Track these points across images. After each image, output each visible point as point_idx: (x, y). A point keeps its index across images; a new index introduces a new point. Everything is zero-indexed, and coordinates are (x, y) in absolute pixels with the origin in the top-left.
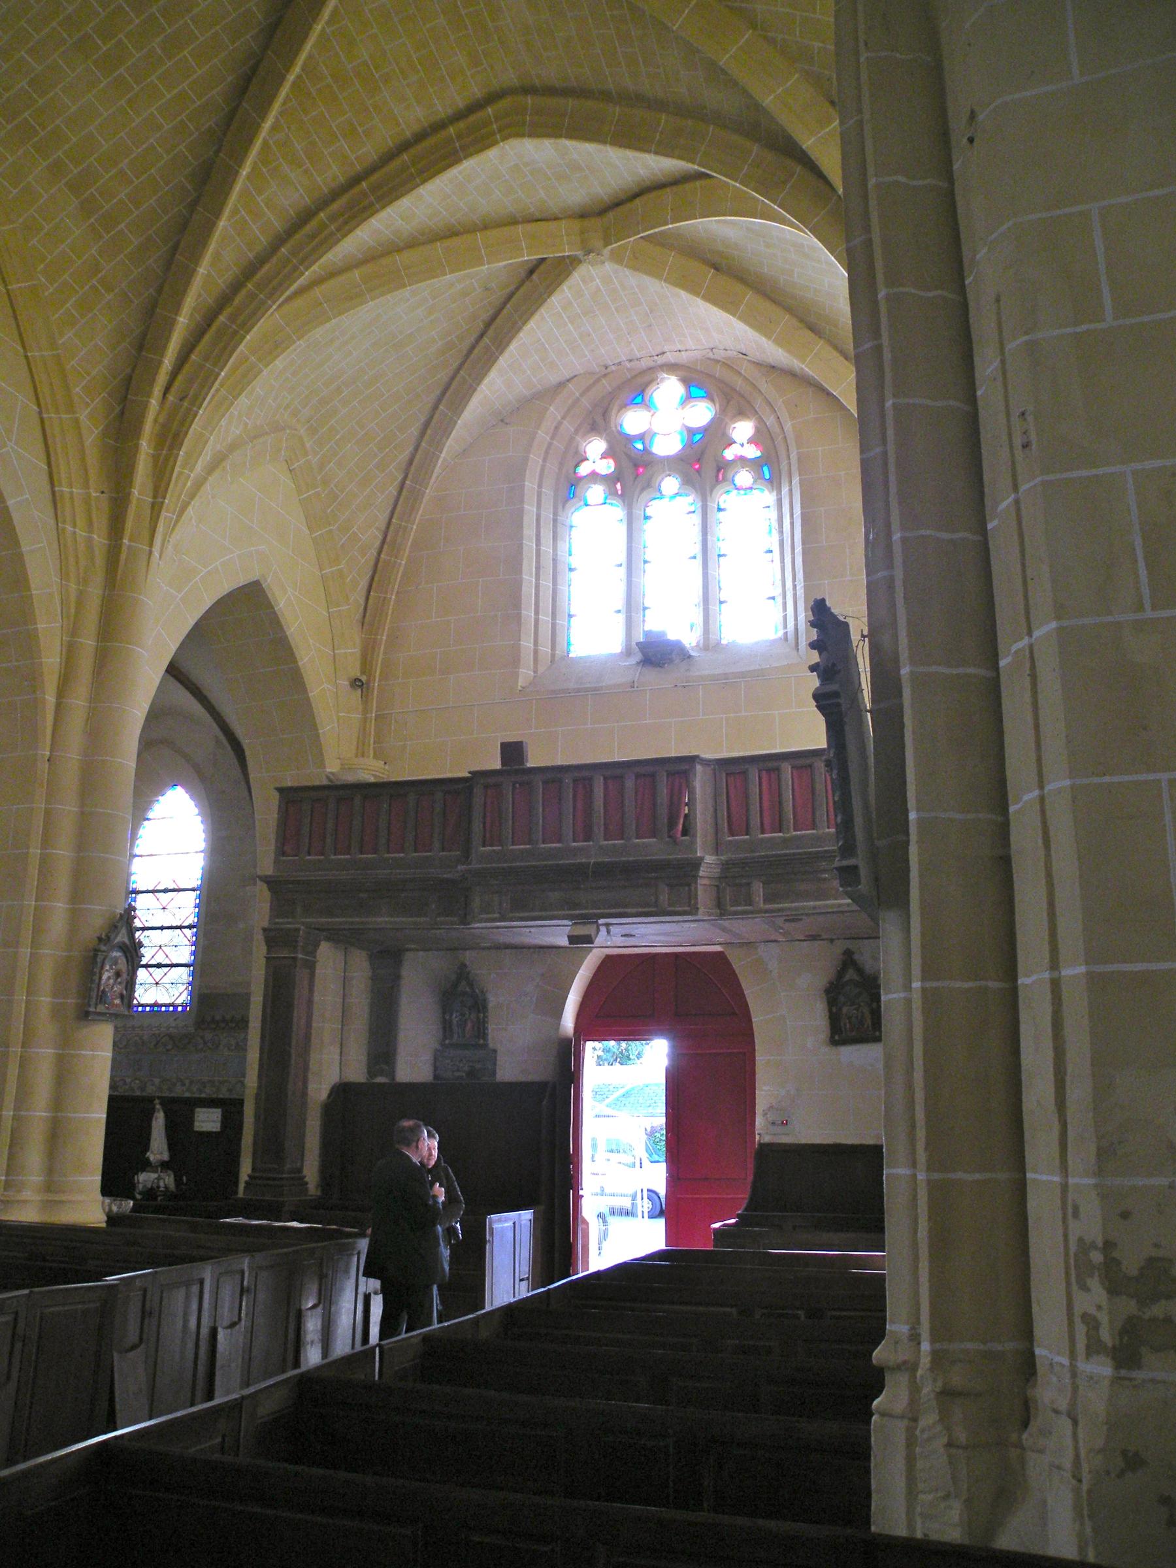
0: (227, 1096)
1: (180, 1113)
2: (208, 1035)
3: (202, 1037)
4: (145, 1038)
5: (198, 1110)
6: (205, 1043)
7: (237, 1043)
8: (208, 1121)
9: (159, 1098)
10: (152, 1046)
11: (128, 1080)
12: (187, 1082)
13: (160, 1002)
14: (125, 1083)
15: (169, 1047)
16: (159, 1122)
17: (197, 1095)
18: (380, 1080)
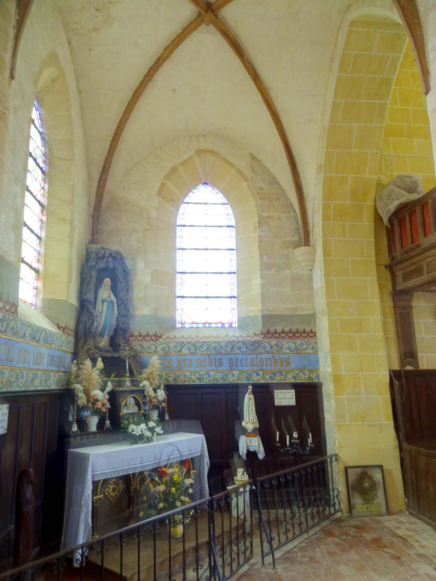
1: (263, 393)
2: (274, 342)
3: (269, 344)
4: (222, 344)
6: (271, 347)
7: (296, 346)
8: (285, 398)
10: (229, 349)
11: (212, 373)
12: (261, 373)
13: (210, 322)
14: (209, 376)
15: (244, 350)
18: (409, 368)
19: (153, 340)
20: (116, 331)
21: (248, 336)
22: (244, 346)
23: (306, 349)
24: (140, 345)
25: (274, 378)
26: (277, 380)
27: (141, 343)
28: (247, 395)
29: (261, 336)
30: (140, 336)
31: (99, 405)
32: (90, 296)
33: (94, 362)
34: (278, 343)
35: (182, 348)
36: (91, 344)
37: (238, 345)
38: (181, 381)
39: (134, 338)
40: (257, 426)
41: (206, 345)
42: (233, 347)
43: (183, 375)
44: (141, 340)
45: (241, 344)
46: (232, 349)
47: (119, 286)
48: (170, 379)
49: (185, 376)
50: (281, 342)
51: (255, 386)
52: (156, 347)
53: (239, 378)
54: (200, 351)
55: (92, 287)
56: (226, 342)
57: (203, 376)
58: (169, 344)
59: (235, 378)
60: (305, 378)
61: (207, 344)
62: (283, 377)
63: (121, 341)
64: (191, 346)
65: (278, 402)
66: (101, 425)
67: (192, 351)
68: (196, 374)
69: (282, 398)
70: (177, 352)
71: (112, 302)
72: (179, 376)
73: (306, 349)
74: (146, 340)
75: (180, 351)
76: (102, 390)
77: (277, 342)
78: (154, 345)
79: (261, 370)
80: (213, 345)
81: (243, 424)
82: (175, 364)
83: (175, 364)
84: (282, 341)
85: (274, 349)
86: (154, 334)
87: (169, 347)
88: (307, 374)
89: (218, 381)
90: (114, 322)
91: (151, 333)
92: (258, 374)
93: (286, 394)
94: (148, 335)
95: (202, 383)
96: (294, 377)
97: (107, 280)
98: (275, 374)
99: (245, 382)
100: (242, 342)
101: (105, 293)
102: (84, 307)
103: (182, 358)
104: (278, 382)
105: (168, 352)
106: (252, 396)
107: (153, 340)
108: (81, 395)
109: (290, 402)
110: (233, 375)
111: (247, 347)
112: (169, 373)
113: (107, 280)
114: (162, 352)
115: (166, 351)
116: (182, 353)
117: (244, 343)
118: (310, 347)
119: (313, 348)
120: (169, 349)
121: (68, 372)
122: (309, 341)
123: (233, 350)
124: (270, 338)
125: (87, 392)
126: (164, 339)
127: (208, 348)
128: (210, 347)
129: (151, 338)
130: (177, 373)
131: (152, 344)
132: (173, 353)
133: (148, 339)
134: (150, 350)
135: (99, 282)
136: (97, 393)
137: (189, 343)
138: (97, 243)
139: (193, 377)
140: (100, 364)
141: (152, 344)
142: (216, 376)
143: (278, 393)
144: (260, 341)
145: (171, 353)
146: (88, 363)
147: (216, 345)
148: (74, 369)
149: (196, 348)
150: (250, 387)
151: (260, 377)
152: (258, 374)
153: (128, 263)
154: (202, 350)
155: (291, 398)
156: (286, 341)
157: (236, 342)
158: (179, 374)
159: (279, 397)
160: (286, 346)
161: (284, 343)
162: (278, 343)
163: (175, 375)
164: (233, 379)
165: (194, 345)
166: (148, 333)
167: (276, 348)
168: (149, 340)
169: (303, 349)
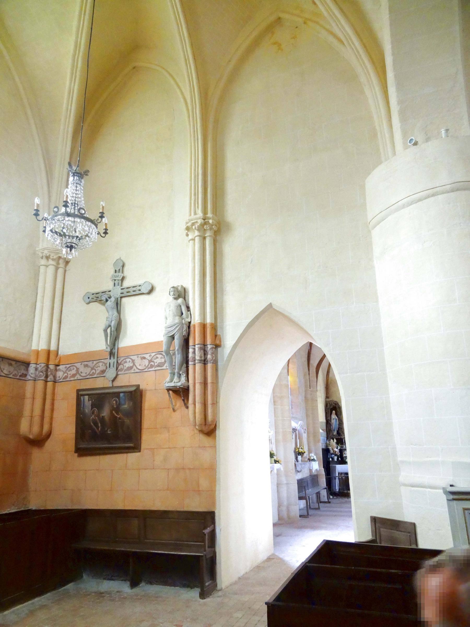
20: (339, 429)
31: (337, 453)
32: (329, 418)
33: (333, 440)
36: (331, 434)
47: (338, 413)
55: (329, 415)
63: (340, 432)
66: (338, 459)
71: (336, 419)
76: (337, 448)
90: (338, 426)
97: (334, 411)
101: (334, 416)
102: (328, 422)
108: (331, 450)
113: (334, 411)
121: (326, 443)
125: (333, 449)
135: (331, 414)
136: (336, 449)
138: (328, 398)
140: (335, 441)
146: (332, 440)
148: (328, 442)
153: (340, 404)
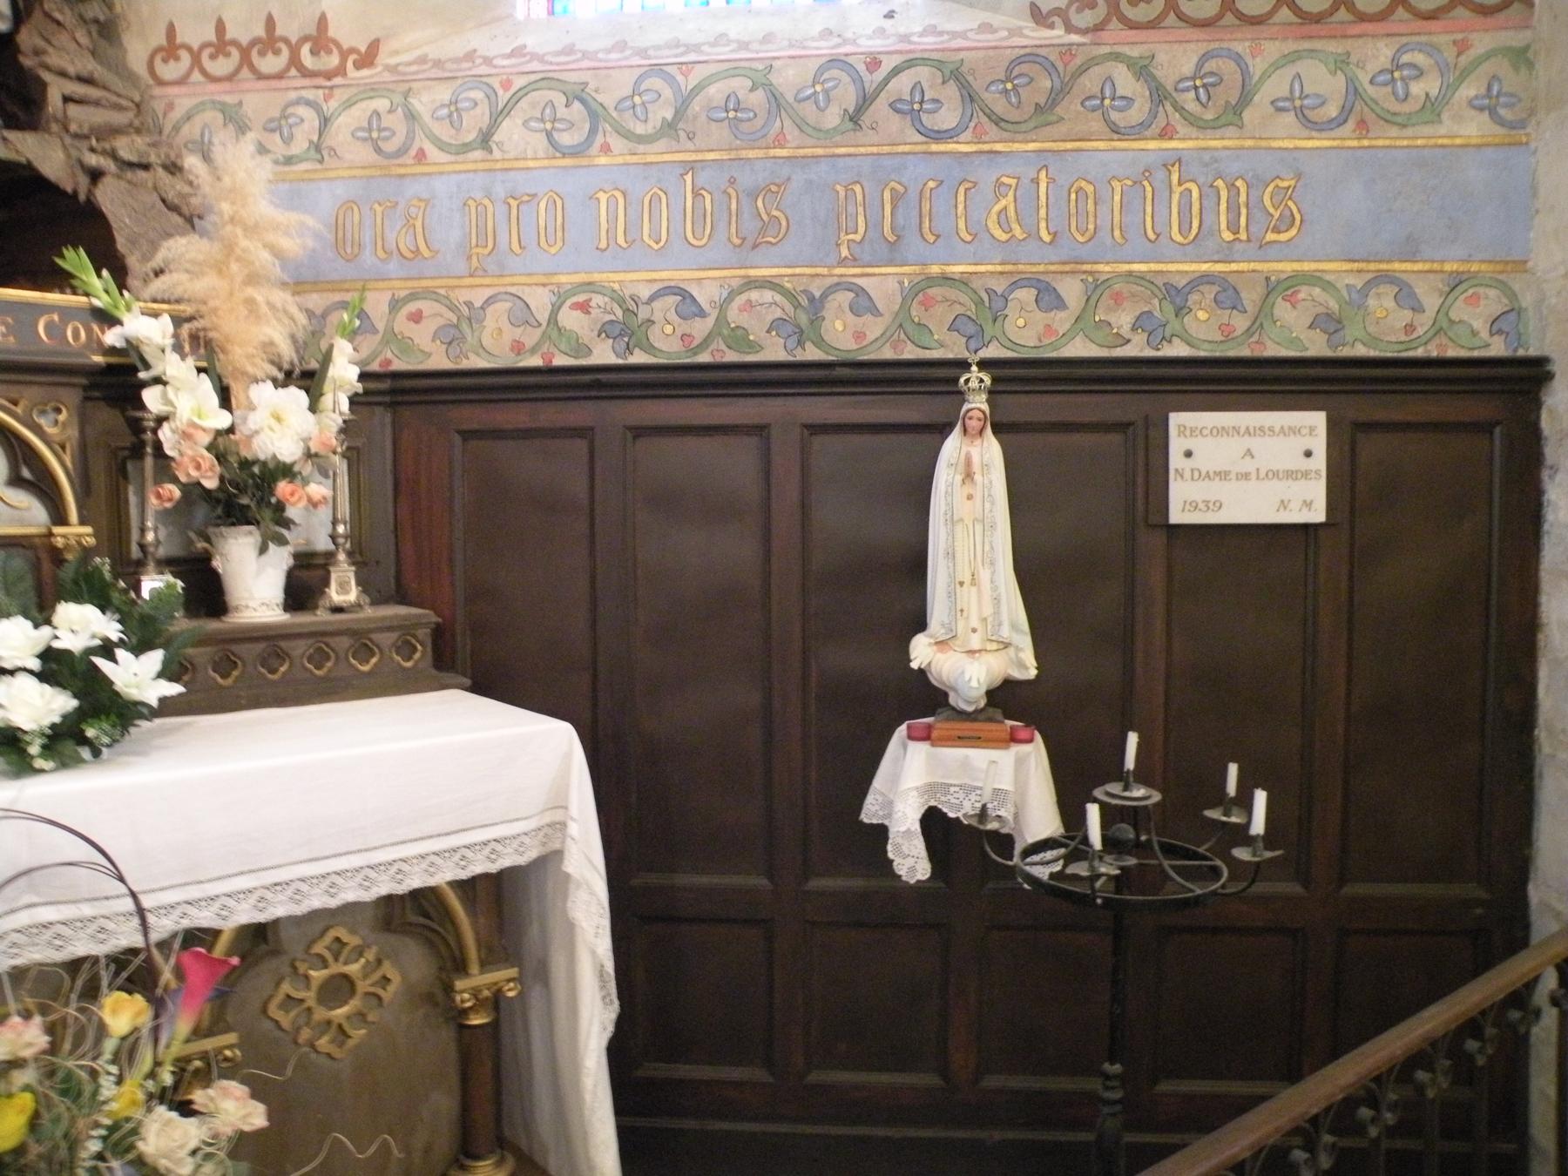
0: (1316, 346)
3: (1142, 70)
4: (788, 79)
5: (1176, 419)
6: (1159, 95)
7: (1353, 90)
8: (1251, 471)
9: (984, 365)
10: (832, 118)
11: (705, 295)
12: (1072, 291)
15: (947, 118)
16: (970, 502)
17: (1137, 348)
19: (306, 73)
21: (986, 28)
22: (952, 90)
23: (1432, 109)
24: (223, 108)
25: (1174, 325)
26: (1201, 334)
27: (230, 99)
28: (952, 446)
29: (1086, 18)
30: (221, 45)
34: (1211, 65)
35: (498, 116)
37: (902, 84)
38: (494, 346)
39: (186, 57)
40: (1028, 668)
41: (667, 93)
42: (866, 100)
43: (502, 306)
44: (230, 78)
45: (923, 74)
46: (854, 118)
48: (422, 335)
49: (523, 315)
50: (1238, 59)
51: (1013, 376)
52: (325, 121)
53: (903, 324)
54: (628, 135)
56: (813, 65)
57: (643, 313)
58: (406, 95)
59: (874, 328)
60: (1409, 328)
61: (670, 80)
62: (1240, 323)
64: (560, 100)
65: (1188, 502)
67: (566, 139)
68: (597, 300)
69: (1223, 475)
70: (466, 148)
72: (474, 316)
73: (1432, 109)
74: (261, 77)
75: (485, 139)
77: (1205, 58)
78: (308, 103)
79: (1073, 266)
80: (716, 92)
81: (921, 651)
82: (449, 234)
83: (449, 234)
84: (1240, 47)
85: (1179, 108)
86: (312, 30)
87: (411, 116)
88: (1431, 303)
89: (739, 337)
91: (289, 28)
92: (1048, 297)
93: (1254, 443)
94: (270, 41)
95: (639, 358)
96: (1329, 323)
98: (1177, 296)
99: (954, 348)
100: (939, 65)
103: (500, 191)
104: (1202, 354)
105: (401, 152)
106: (990, 452)
107: (306, 73)
109: (1283, 505)
110: (863, 303)
111: (970, 96)
112: (413, 297)
114: (365, 154)
115: (389, 147)
116: (497, 154)
117: (954, 73)
118: (1469, 90)
119: (1488, 106)
120: (410, 137)
122: (1462, 47)
123: (866, 120)
124: (1152, 25)
126: (392, 69)
127: (679, 113)
128: (696, 106)
129: (295, 61)
130: (462, 296)
131: (298, 102)
132: (433, 153)
133: (270, 63)
134: (288, 141)
137: (547, 81)
139: (570, 319)
141: (298, 102)
142: (734, 316)
143: (1194, 432)
144: (1068, 51)
145: (421, 155)
147: (740, 85)
149: (595, 115)
150: (976, 378)
151: (1062, 321)
152: (1048, 297)
154: (640, 129)
155: (1291, 475)
156: (1274, 49)
157: (888, 64)
158: (478, 298)
159: (1201, 461)
160: (1278, 86)
161: (1257, 66)
162: (1211, 65)
163: (452, 308)
164: (859, 336)
165: (578, 95)
166: (270, 23)
167: (1192, 106)
168: (280, 76)
169: (1406, 108)
